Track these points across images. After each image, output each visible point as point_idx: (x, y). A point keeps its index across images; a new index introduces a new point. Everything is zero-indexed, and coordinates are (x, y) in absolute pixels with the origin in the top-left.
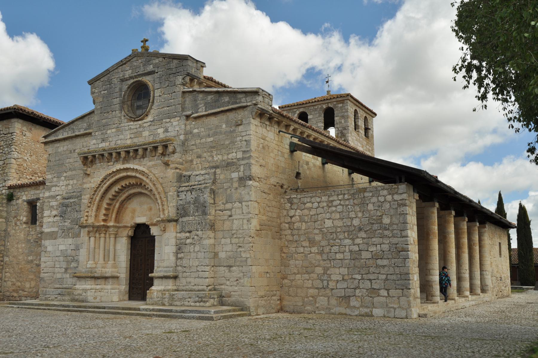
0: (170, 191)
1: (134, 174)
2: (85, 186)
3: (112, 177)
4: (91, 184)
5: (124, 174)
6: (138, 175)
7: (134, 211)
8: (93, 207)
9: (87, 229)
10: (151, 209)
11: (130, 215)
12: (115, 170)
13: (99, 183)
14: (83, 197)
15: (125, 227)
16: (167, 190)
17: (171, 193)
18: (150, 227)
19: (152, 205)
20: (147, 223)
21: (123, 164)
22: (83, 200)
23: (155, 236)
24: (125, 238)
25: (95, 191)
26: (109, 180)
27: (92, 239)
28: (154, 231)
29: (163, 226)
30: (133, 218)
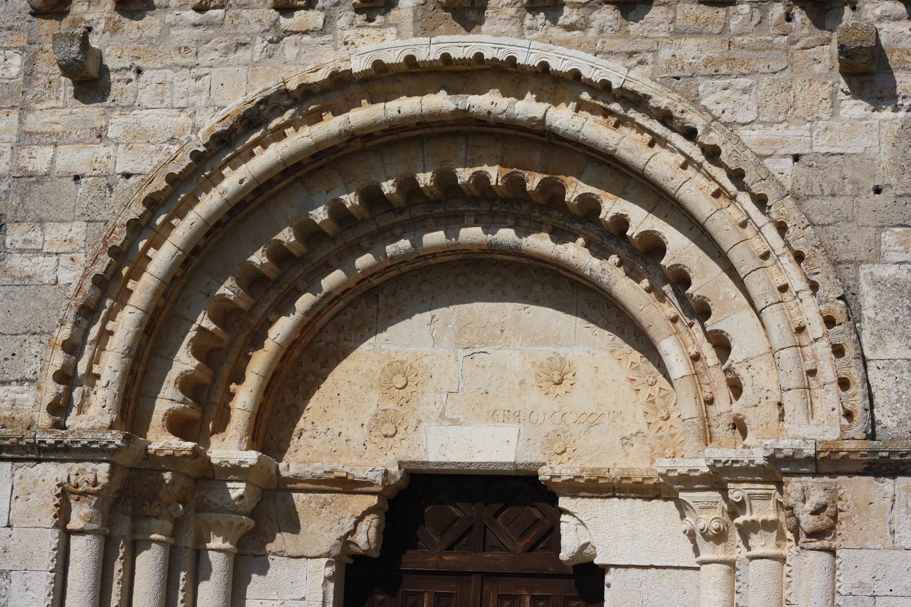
0: (877, 257)
1: (527, 107)
2: (40, 159)
3: (315, 118)
4: (101, 150)
5: (440, 101)
6: (563, 117)
7: (401, 380)
8: (111, 315)
9: (52, 473)
10: (558, 377)
11: (373, 402)
12: (359, 65)
13: (199, 142)
14: (15, 235)
15: (347, 485)
16: (854, 243)
17: (887, 272)
18: (564, 502)
19: (574, 353)
20: (544, 474)
21: (425, 28)
22: (16, 262)
23: (603, 570)
24: (321, 569)
25: (153, 203)
26: (279, 134)
27: (83, 551)
28: (585, 529)
29: (817, 497)
30: (387, 427)
